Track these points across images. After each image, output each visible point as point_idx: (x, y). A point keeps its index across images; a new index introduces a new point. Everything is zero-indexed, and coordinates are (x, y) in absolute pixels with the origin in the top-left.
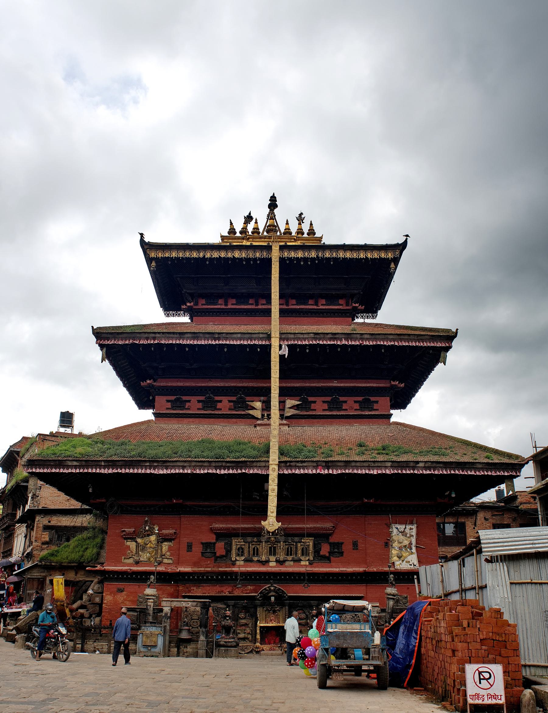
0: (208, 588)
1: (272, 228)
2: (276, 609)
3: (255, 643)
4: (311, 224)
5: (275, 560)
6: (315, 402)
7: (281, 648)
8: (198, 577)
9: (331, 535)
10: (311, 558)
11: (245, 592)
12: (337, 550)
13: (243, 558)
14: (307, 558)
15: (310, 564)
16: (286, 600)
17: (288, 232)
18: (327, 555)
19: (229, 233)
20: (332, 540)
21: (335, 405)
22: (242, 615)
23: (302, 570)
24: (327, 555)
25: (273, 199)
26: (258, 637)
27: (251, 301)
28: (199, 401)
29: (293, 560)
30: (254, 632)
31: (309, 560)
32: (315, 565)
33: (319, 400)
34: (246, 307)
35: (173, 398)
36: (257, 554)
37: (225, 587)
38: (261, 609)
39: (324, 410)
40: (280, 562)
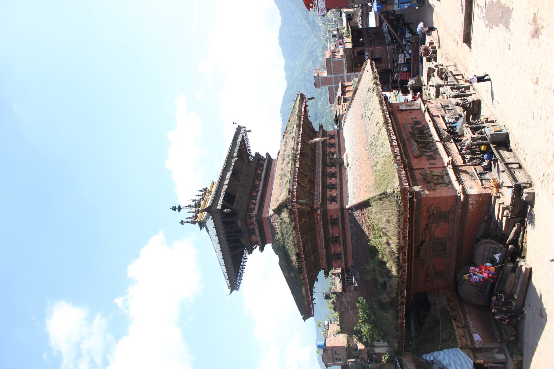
4: (200, 191)
19: (195, 223)
25: (174, 209)
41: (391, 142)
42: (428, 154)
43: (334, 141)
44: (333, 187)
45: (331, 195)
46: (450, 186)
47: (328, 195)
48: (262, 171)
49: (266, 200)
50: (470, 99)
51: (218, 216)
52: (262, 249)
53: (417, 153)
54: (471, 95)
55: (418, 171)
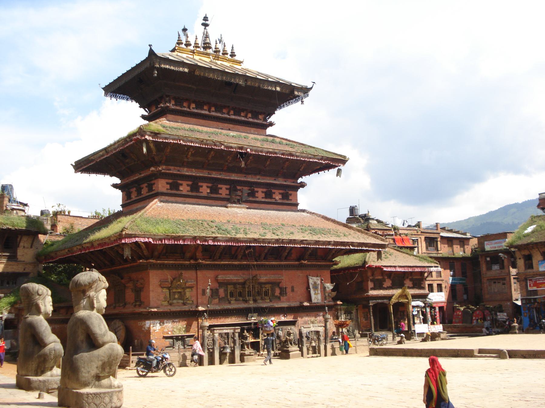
1: (207, 46)
4: (233, 48)
6: (257, 192)
9: (280, 283)
12: (283, 292)
13: (234, 299)
15: (271, 301)
17: (217, 51)
18: (279, 295)
20: (281, 285)
21: (268, 195)
24: (279, 295)
25: (206, 19)
27: (205, 108)
28: (188, 185)
29: (262, 299)
33: (260, 190)
34: (203, 112)
35: (170, 181)
39: (263, 198)
40: (255, 301)
41: (200, 238)
42: (221, 291)
43: (277, 198)
44: (195, 188)
45: (182, 185)
46: (166, 303)
47: (180, 182)
48: (246, 116)
49: (194, 120)
50: (294, 349)
51: (147, 65)
52: (143, 117)
53: (220, 278)
54: (301, 350)
55: (195, 275)
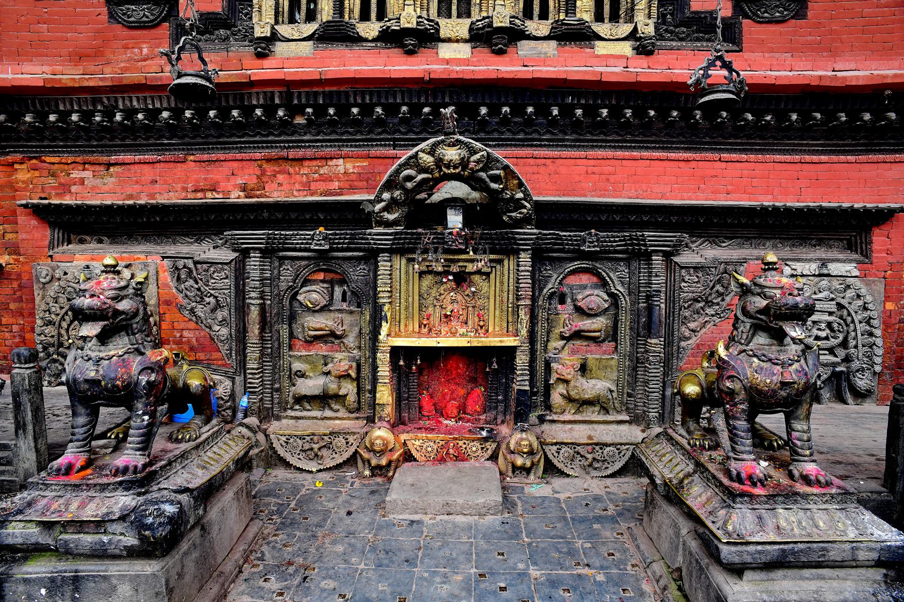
0: (148, 173)
2: (471, 268)
3: (371, 420)
5: (465, 34)
7: (491, 446)
8: (87, 116)
10: (647, 28)
11: (322, 186)
14: (625, 29)
16: (524, 221)
22: (313, 295)
23: (613, 72)
26: (385, 395)
30: (366, 371)
31: (632, 35)
32: (661, 57)
36: (381, 16)
37: (227, 168)
38: (400, 263)
